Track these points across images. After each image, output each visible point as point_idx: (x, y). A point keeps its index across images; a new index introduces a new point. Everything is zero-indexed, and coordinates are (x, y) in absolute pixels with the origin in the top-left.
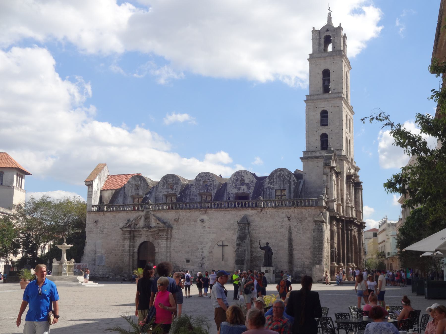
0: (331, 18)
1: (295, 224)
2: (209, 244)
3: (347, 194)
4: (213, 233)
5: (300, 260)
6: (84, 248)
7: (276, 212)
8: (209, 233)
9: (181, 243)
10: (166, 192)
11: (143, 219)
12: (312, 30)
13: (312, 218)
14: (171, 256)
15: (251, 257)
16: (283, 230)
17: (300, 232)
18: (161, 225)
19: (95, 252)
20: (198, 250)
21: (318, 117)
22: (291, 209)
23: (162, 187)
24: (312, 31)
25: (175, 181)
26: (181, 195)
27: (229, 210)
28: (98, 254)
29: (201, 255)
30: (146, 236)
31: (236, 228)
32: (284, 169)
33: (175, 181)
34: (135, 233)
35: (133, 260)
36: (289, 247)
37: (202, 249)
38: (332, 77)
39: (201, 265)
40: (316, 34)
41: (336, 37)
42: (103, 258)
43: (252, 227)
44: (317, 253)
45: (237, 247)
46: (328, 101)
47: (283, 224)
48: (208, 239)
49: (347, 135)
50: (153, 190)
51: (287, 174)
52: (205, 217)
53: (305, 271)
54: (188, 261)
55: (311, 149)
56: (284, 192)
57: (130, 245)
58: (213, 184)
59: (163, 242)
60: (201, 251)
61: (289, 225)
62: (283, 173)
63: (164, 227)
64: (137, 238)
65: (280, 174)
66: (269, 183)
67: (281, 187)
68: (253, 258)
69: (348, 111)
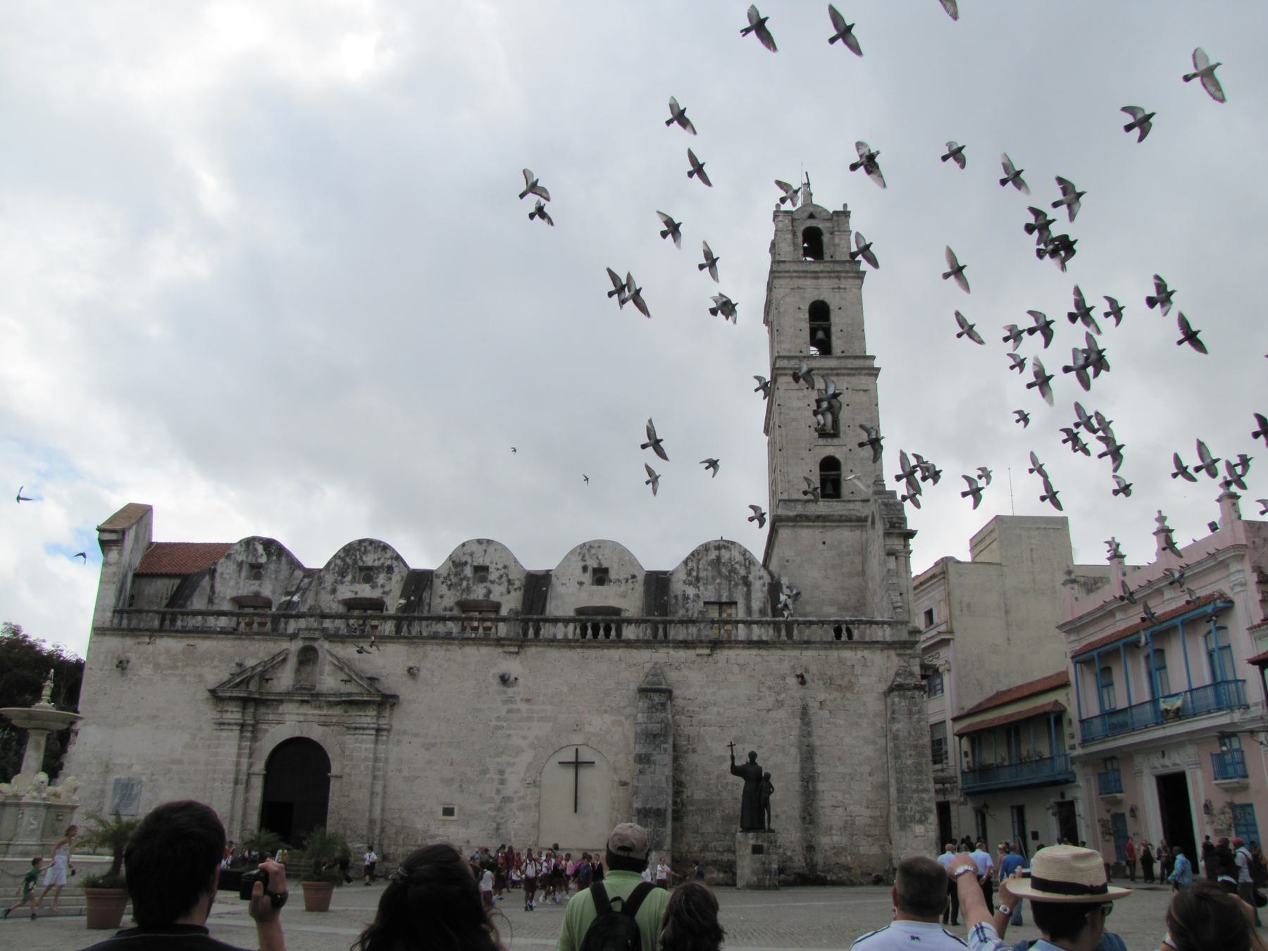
0: (811, 195)
1: (822, 697)
2: (528, 757)
4: (541, 719)
5: (840, 811)
6: (66, 751)
7: (759, 659)
8: (529, 719)
9: (427, 749)
10: (352, 591)
11: (292, 662)
13: (874, 679)
14: (385, 793)
15: (675, 803)
16: (781, 714)
17: (842, 722)
19: (107, 766)
20: (488, 776)
22: (806, 649)
23: (339, 578)
25: (382, 560)
26: (408, 599)
27: (598, 647)
28: (118, 776)
29: (498, 791)
30: (299, 722)
31: (622, 704)
32: (733, 543)
33: (382, 560)
34: (263, 710)
35: (246, 800)
36: (803, 769)
37: (502, 772)
39: (494, 825)
40: (787, 221)
41: (836, 233)
42: (132, 789)
43: (679, 702)
44: (914, 786)
45: (640, 766)
46: (837, 375)
47: (783, 696)
48: (524, 738)
50: (310, 583)
51: (739, 558)
52: (513, 666)
53: (858, 846)
54: (448, 812)
56: (729, 611)
57: (240, 748)
58: (507, 576)
59: (361, 743)
60: (500, 777)
61: (803, 699)
62: (725, 555)
63: (369, 693)
64: (264, 726)
65: (719, 558)
66: (684, 582)
67: (720, 596)
68: (680, 806)
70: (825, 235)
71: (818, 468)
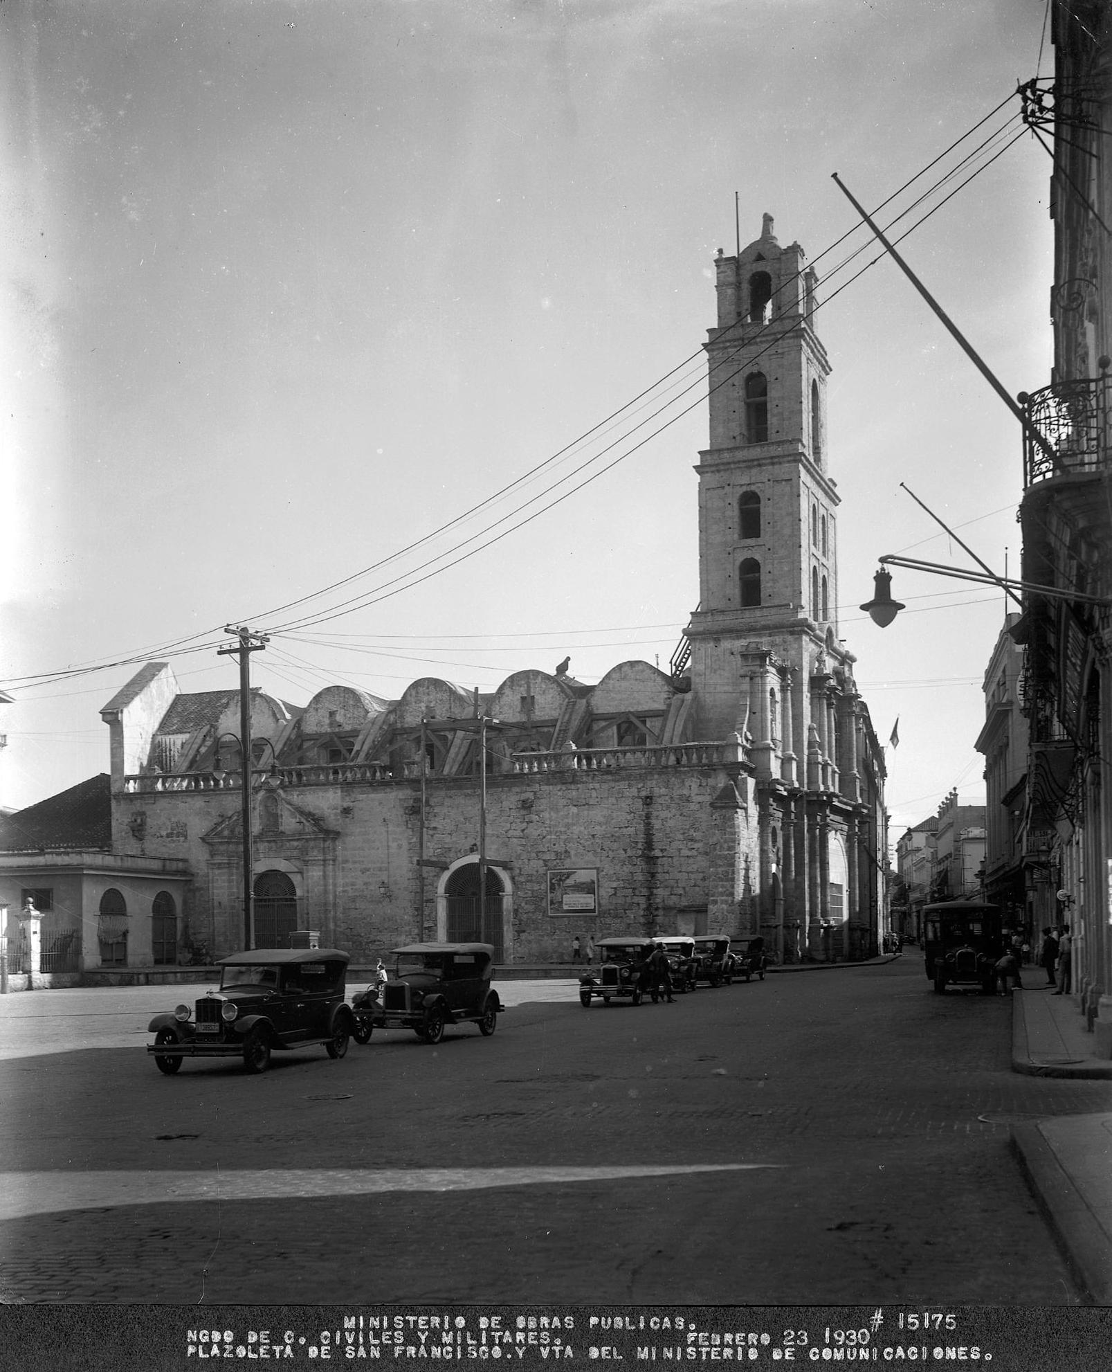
3: (810, 729)
12: (716, 257)
18: (309, 827)
21: (734, 513)
24: (716, 261)
38: (774, 393)
46: (760, 465)
49: (814, 562)
55: (714, 605)
69: (820, 494)
70: (773, 280)
71: (737, 572)
